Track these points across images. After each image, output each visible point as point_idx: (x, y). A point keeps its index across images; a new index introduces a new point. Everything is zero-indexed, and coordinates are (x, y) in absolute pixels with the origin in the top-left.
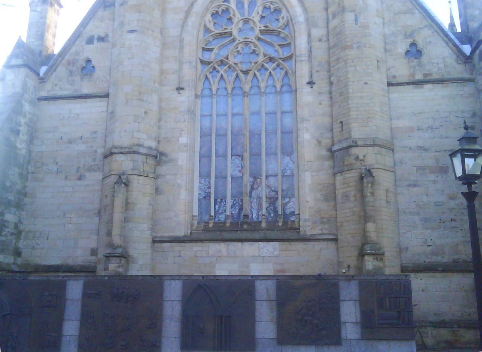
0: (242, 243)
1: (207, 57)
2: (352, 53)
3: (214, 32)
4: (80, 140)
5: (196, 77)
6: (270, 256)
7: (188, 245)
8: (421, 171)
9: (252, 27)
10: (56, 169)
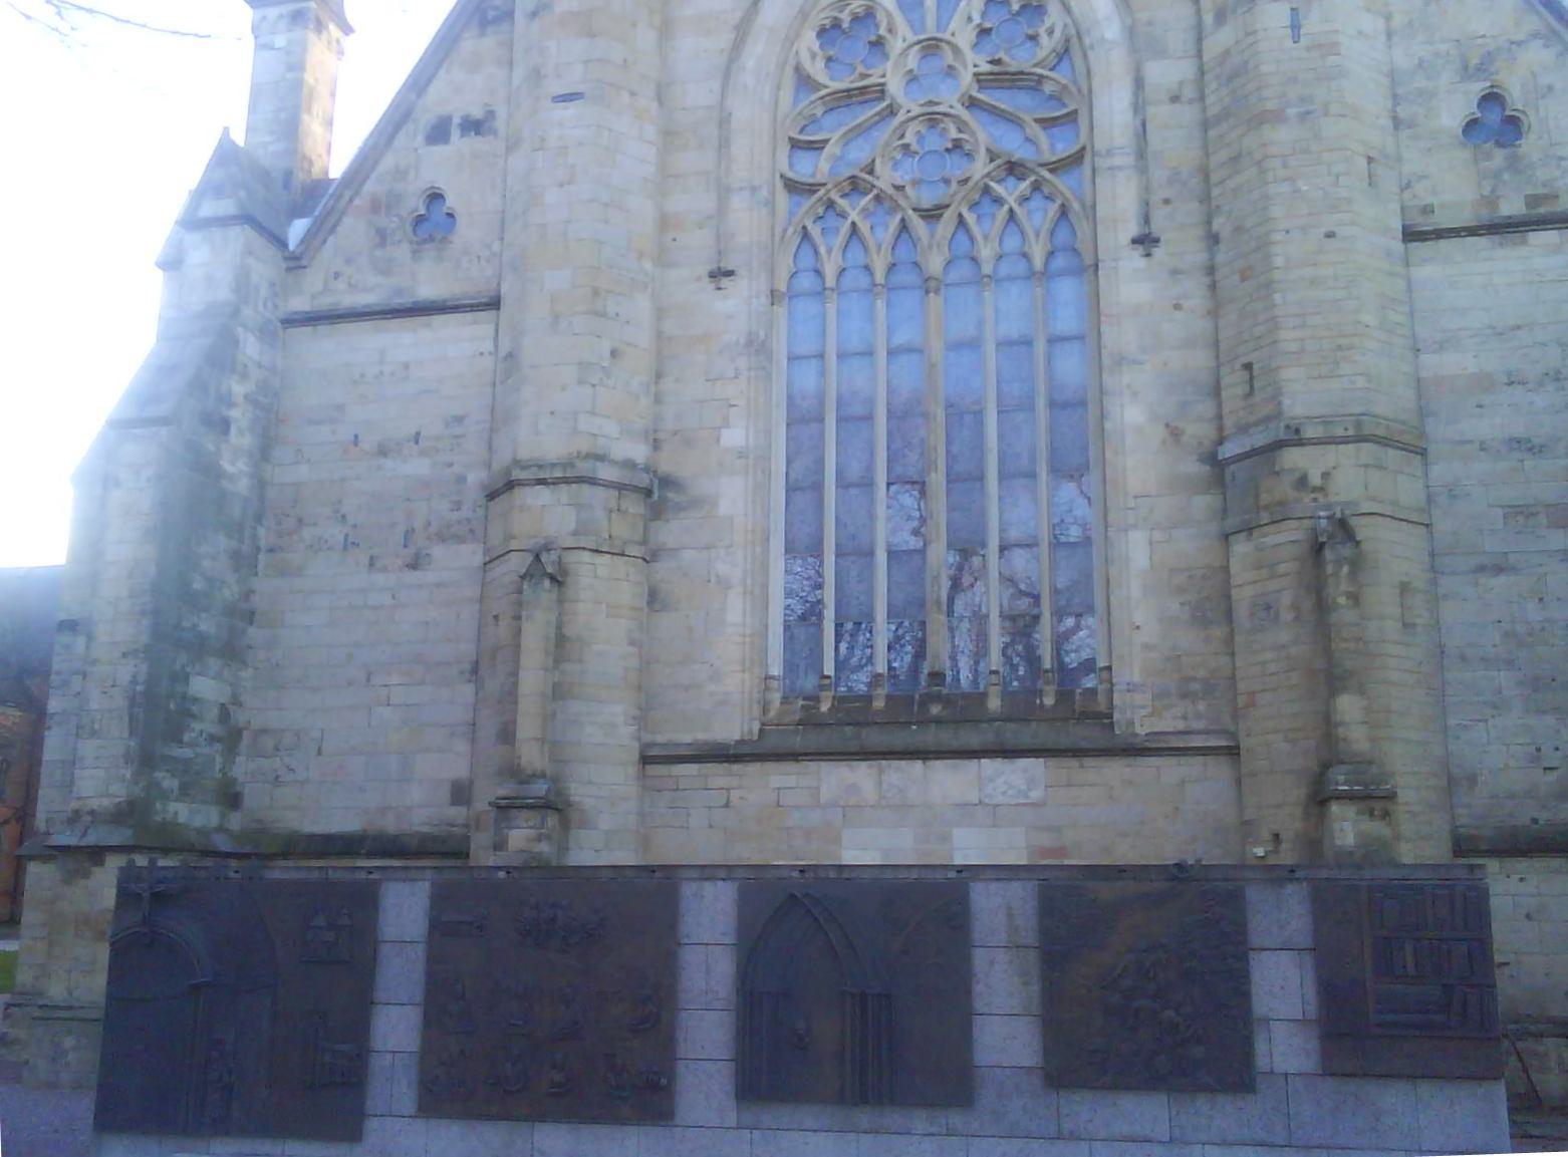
0: (924, 763)
1: (808, 168)
2: (1280, 136)
3: (826, 87)
4: (412, 444)
5: (773, 235)
7: (753, 768)
9: (950, 67)
10: (341, 538)
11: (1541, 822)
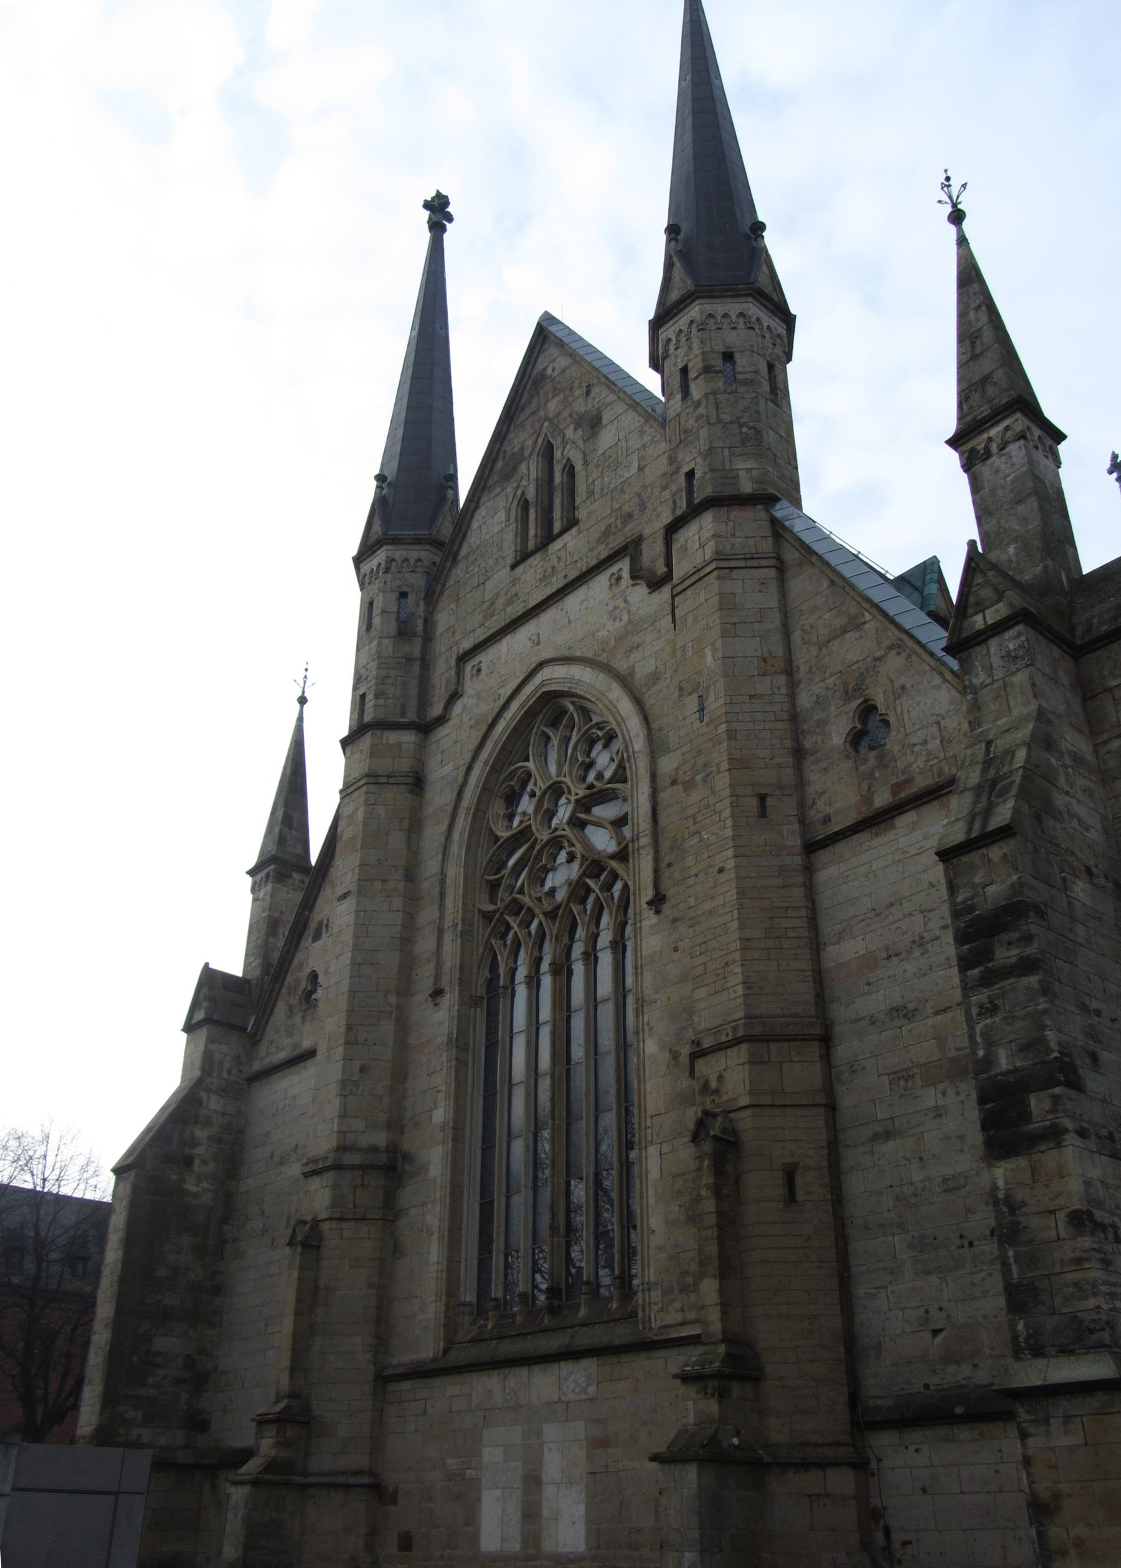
6: (580, 1401)
8: (902, 1082)
11: (932, 1388)
